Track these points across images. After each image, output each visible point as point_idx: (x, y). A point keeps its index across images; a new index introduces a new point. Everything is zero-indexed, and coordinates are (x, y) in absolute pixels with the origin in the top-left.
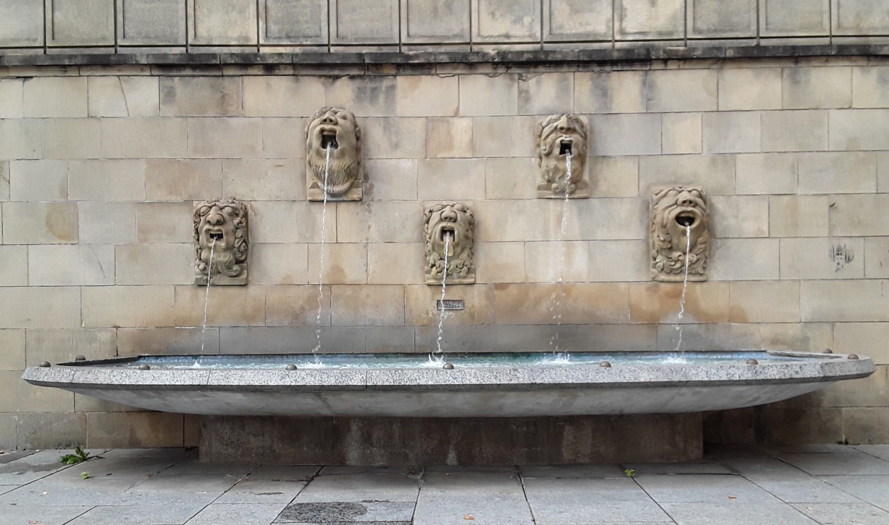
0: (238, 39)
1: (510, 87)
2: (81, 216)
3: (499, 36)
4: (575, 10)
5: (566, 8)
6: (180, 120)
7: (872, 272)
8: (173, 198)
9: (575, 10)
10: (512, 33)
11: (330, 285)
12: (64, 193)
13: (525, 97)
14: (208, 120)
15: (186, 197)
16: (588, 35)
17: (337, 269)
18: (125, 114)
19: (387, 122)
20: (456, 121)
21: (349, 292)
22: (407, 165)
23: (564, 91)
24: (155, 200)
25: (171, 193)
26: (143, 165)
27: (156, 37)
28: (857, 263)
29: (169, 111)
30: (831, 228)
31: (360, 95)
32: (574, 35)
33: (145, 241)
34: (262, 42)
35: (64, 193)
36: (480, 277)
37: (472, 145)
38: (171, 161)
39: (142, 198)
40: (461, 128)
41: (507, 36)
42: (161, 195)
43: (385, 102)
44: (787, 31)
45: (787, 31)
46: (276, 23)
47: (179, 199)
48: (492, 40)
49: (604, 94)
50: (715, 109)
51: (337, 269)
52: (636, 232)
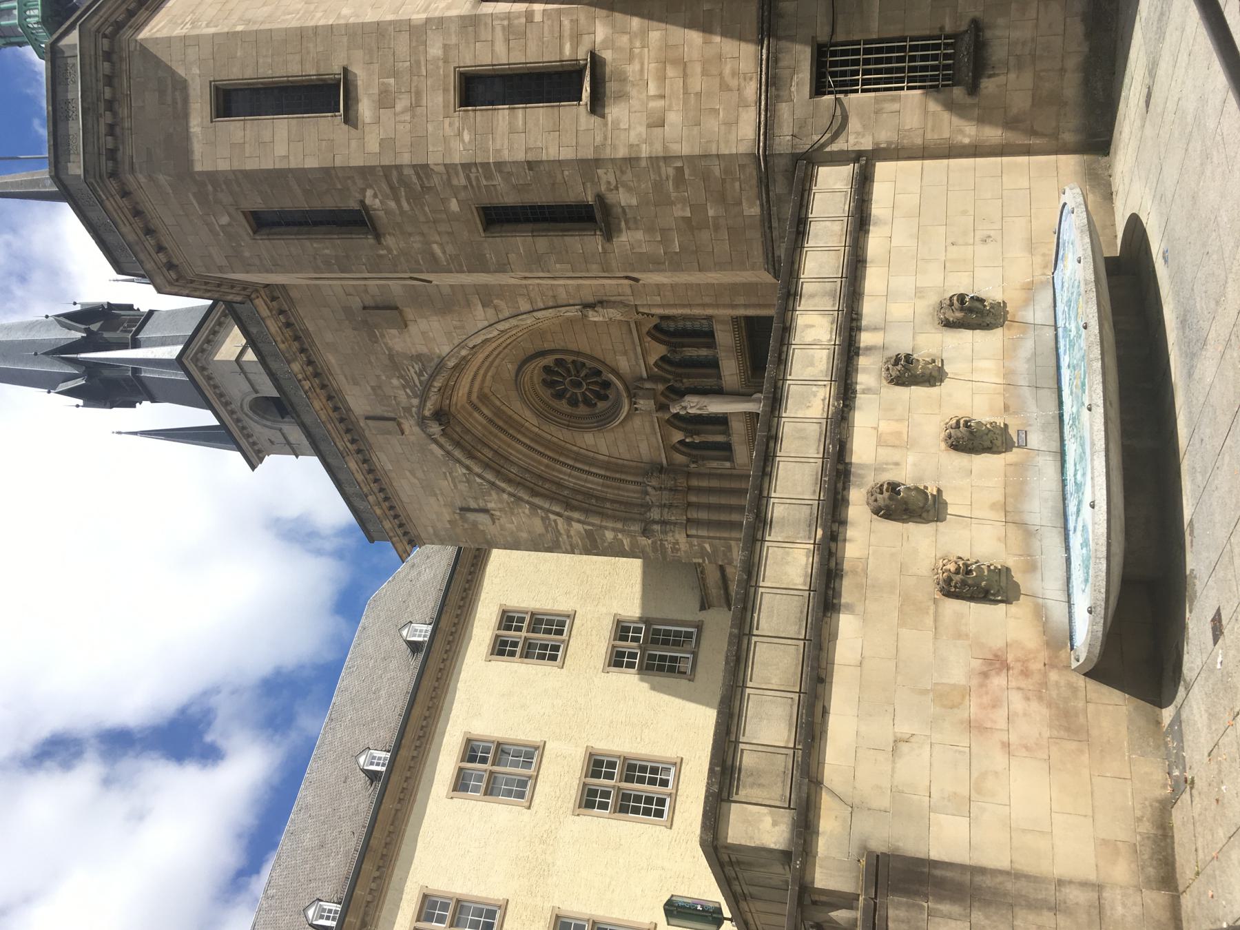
0: (808, 557)
1: (860, 398)
2: (944, 681)
3: (824, 404)
4: (812, 364)
5: (810, 368)
6: (867, 602)
7: (998, 226)
8: (932, 611)
9: (812, 364)
10: (822, 398)
11: (1005, 511)
12: (924, 692)
13: (867, 391)
14: (869, 582)
15: (931, 603)
16: (828, 358)
17: (993, 506)
18: (861, 640)
19: (879, 469)
20: (879, 429)
21: (1010, 500)
22: (911, 458)
23: (866, 370)
24: (932, 623)
25: (927, 613)
26: (904, 632)
27: (802, 612)
28: (992, 233)
29: (859, 608)
30: (967, 244)
31: (860, 486)
32: (828, 363)
33: (967, 635)
34: (812, 542)
35: (924, 692)
36: (1000, 422)
37: (899, 420)
38: (901, 611)
39: (931, 634)
40: (884, 426)
41: (823, 400)
42: (929, 621)
43: (863, 469)
44: (839, 267)
45: (839, 267)
46: (799, 533)
47: (932, 607)
48: (826, 407)
49: (869, 349)
50: (885, 298)
51: (993, 506)
52: (966, 335)
